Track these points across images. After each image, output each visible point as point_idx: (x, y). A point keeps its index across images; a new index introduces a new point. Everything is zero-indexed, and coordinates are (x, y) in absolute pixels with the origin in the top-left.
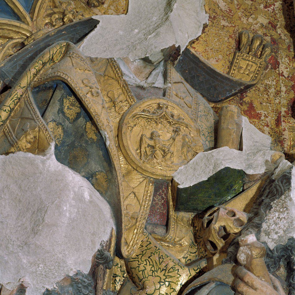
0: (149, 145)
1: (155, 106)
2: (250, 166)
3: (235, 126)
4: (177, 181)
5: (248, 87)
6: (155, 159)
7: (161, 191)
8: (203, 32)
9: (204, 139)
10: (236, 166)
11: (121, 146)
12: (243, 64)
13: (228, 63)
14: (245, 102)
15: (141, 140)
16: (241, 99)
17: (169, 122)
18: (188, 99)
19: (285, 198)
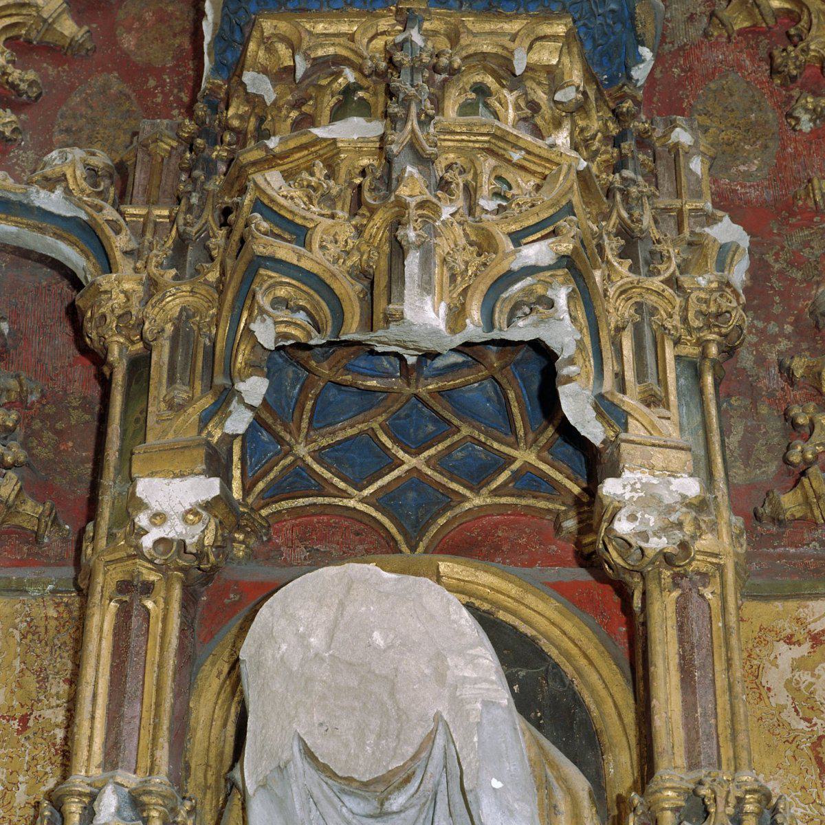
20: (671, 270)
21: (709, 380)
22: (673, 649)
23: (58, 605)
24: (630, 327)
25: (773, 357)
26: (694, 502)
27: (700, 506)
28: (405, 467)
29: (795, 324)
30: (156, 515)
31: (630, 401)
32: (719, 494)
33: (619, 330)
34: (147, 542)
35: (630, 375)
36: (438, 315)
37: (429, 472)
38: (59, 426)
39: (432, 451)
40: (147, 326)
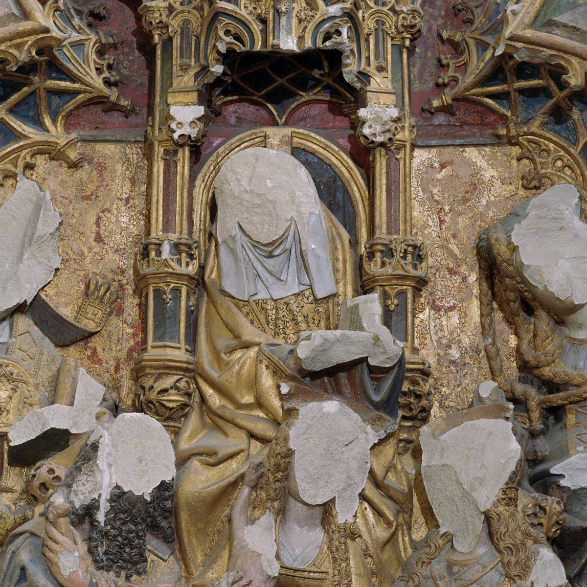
2: (75, 424)
3: (71, 379)
4: (10, 438)
5: (92, 334)
8: (55, 275)
9: (43, 390)
12: (90, 310)
13: (76, 307)
14: (89, 347)
16: (86, 344)
17: (8, 380)
18: (33, 351)
20: (392, 3)
21: (405, 56)
22: (384, 181)
23: (137, 148)
24: (374, 32)
25: (435, 27)
26: (396, 119)
27: (397, 120)
28: (278, 83)
29: (446, 11)
30: (179, 123)
31: (372, 70)
32: (406, 113)
33: (369, 35)
34: (176, 136)
35: (372, 58)
36: (293, 43)
37: (288, 85)
38: (131, 58)
39: (289, 76)
40: (170, 30)
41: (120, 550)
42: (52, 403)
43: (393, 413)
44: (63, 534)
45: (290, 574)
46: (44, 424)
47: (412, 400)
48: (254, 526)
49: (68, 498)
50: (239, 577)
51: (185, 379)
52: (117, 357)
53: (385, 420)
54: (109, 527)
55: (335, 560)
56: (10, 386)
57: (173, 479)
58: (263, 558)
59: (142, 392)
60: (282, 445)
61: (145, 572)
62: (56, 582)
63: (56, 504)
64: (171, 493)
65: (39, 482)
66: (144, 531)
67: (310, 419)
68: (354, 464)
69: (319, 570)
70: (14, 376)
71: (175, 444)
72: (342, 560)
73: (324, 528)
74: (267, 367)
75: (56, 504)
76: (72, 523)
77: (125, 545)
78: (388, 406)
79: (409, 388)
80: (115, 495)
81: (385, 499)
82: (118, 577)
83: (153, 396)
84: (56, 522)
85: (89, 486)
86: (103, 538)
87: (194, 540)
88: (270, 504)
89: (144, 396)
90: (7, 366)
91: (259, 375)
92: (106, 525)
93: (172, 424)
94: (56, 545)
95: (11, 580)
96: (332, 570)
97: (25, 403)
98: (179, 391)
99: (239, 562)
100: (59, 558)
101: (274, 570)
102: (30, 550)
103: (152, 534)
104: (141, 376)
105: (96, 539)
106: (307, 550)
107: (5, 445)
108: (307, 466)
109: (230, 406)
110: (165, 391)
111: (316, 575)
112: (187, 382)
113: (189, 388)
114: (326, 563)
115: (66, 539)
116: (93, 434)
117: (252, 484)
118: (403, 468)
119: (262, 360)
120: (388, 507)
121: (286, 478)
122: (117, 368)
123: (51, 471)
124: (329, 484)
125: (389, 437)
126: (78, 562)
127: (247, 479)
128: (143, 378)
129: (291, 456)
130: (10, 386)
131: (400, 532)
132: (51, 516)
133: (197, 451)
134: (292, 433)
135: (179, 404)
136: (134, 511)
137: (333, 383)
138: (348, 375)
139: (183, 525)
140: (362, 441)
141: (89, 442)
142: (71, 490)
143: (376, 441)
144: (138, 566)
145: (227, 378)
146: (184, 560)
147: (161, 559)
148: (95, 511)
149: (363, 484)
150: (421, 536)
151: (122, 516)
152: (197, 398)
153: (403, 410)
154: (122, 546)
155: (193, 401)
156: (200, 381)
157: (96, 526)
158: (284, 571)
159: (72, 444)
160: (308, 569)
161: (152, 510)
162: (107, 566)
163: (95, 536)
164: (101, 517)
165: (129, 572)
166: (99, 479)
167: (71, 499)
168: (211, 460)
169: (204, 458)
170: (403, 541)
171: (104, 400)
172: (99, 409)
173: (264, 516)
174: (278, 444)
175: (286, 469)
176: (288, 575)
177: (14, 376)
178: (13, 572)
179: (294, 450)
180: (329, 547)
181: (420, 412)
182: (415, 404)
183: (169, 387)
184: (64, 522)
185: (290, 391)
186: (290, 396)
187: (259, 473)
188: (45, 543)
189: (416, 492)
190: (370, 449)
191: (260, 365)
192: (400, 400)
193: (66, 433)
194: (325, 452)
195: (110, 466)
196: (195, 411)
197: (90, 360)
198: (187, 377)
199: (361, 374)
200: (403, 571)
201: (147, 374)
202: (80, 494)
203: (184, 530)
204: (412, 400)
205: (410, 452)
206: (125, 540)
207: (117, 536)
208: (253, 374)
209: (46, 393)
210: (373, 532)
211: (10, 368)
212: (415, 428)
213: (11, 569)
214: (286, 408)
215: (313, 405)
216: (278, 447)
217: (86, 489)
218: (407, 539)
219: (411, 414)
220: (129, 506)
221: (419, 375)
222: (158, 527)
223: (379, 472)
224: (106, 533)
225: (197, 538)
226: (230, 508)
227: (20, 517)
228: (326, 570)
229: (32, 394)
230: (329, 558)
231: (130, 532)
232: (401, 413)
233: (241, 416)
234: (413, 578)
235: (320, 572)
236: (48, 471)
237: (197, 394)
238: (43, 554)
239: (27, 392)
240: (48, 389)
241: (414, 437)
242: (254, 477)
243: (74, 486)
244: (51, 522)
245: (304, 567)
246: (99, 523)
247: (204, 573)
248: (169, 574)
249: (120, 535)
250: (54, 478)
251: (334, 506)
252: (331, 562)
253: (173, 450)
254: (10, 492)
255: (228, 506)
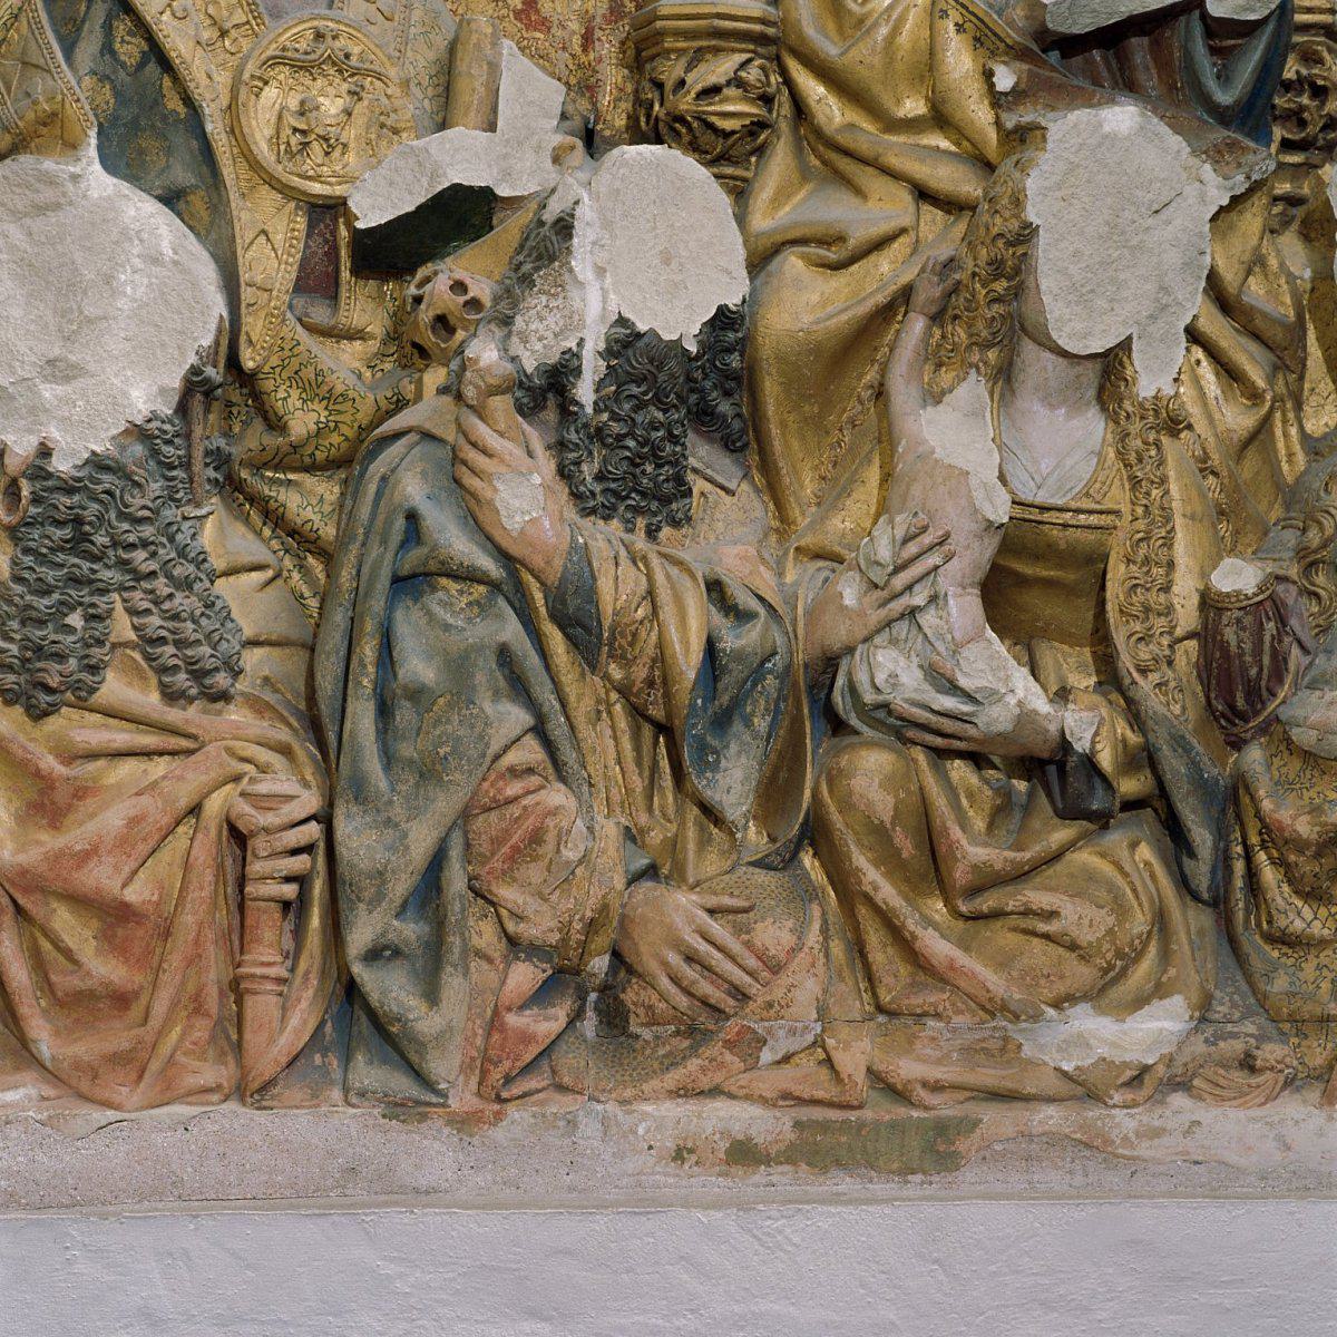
0: (295, 130)
1: (310, 35)
2: (507, 174)
3: (485, 67)
4: (354, 210)
6: (308, 161)
7: (322, 226)
9: (420, 96)
10: (475, 178)
11: (237, 132)
15: (280, 117)
17: (340, 71)
19: (561, 267)
41: (631, 469)
42: (443, 125)
43: (1260, 134)
44: (501, 435)
45: (1032, 517)
46: (433, 177)
47: (1305, 100)
48: (941, 407)
49: (506, 350)
50: (919, 525)
51: (758, 62)
52: (587, 11)
53: (1244, 149)
54: (605, 416)
55: (1135, 483)
56: (345, 86)
57: (744, 301)
58: (973, 482)
59: (657, 95)
60: (1007, 214)
61: (689, 519)
62: (489, 545)
63: (482, 364)
64: (740, 335)
65: (431, 314)
66: (683, 425)
67: (1073, 150)
68: (1173, 258)
69: (1098, 507)
70: (354, 61)
71: (741, 219)
72: (1153, 482)
73: (1104, 408)
74: (960, 28)
75: (482, 364)
76: (520, 409)
77: (643, 457)
78: (1250, 117)
79: (1297, 72)
80: (617, 341)
81: (1244, 340)
82: (631, 531)
83: (686, 103)
84: (484, 408)
85: (553, 321)
86: (592, 443)
87: (795, 444)
88: (977, 357)
89: (662, 105)
90: (335, 38)
91: (938, 47)
92: (597, 410)
93: (729, 170)
94: (487, 460)
95: (384, 542)
96: (1129, 505)
97: (382, 126)
98: (746, 91)
99: (916, 491)
100: (496, 490)
101: (1000, 510)
102: (424, 474)
103: (697, 432)
104: (652, 58)
105: (577, 445)
106: (1069, 462)
107: (342, 227)
108: (1066, 264)
109: (867, 125)
110: (712, 91)
111: (1093, 520)
112: (762, 68)
113: (769, 84)
114: (1115, 490)
115: (509, 445)
116: (555, 197)
117: (934, 309)
118: (1282, 265)
119: (946, 12)
120: (1252, 357)
121: (1016, 295)
122: (588, 40)
123: (459, 287)
124: (1116, 306)
125: (1251, 191)
126: (541, 498)
127: (921, 297)
128: (658, 61)
129: (1029, 241)
130: (345, 86)
131: (1278, 415)
132: (470, 393)
133: (790, 236)
134: (1032, 184)
135: (748, 122)
136: (662, 377)
137: (1114, 63)
138: (1151, 44)
139: (770, 409)
140: (1190, 201)
141: (549, 216)
142: (510, 332)
143: (1225, 202)
144: (674, 506)
145: (860, 58)
146: (773, 490)
147: (722, 488)
148: (571, 379)
149: (1194, 305)
150: (1326, 424)
151: (635, 390)
152: (784, 107)
153: (1284, 127)
154: (638, 460)
155: (778, 114)
156: (794, 66)
157: (576, 414)
158: (1018, 512)
159: (502, 221)
160: (1073, 505)
161: (698, 375)
162: (603, 505)
163: (573, 437)
164: (585, 392)
165: (655, 521)
166: (577, 304)
167: (512, 353)
168: (832, 255)
169: (812, 250)
170: (1286, 439)
171: (564, 116)
172: (558, 139)
173: (964, 384)
174: (996, 212)
175: (1017, 271)
176: (1025, 520)
177: (354, 61)
178: (389, 523)
179: (1038, 226)
180: (1119, 452)
181: (1324, 129)
182: (1314, 110)
183: (722, 80)
184: (501, 405)
185: (1017, 84)
186: (1018, 95)
187: (950, 282)
188: (461, 455)
189: (1314, 322)
190: (1214, 219)
191: (940, 24)
192: (1277, 101)
193: (486, 195)
194: (1106, 229)
195: (600, 271)
196: (782, 140)
197: (521, 20)
198: (762, 57)
199: (1186, 41)
200: (1288, 506)
201: (669, 51)
202: (533, 339)
203: (772, 420)
204: (1305, 100)
205: (1295, 226)
206: (642, 445)
207: (625, 436)
208: (924, 45)
209: (426, 101)
210: (1217, 416)
211: (341, 43)
212: (1310, 167)
213: (381, 517)
214: (1009, 125)
215: (1080, 116)
216: (998, 220)
217: (548, 328)
218: (1293, 431)
219: (1303, 135)
220: (649, 367)
221: (1322, 39)
222: (712, 414)
223: (1230, 276)
224: (599, 430)
225: (803, 438)
226: (876, 367)
227: (389, 396)
228: (1116, 507)
229: (398, 103)
230: (1121, 479)
231: (654, 426)
232: (1278, 133)
233: (897, 150)
234: (1319, 523)
235: (1101, 512)
236: (451, 288)
237: (785, 95)
238: (456, 481)
239: (384, 100)
240: (430, 92)
241: (1306, 191)
242: (937, 292)
243: (519, 320)
244: (470, 407)
245: (1064, 500)
246: (582, 406)
247: (823, 519)
248: (743, 524)
249: (631, 434)
250: (466, 303)
251: (1129, 357)
252: (1127, 486)
253: (738, 233)
254: (360, 339)
255: (873, 361)
